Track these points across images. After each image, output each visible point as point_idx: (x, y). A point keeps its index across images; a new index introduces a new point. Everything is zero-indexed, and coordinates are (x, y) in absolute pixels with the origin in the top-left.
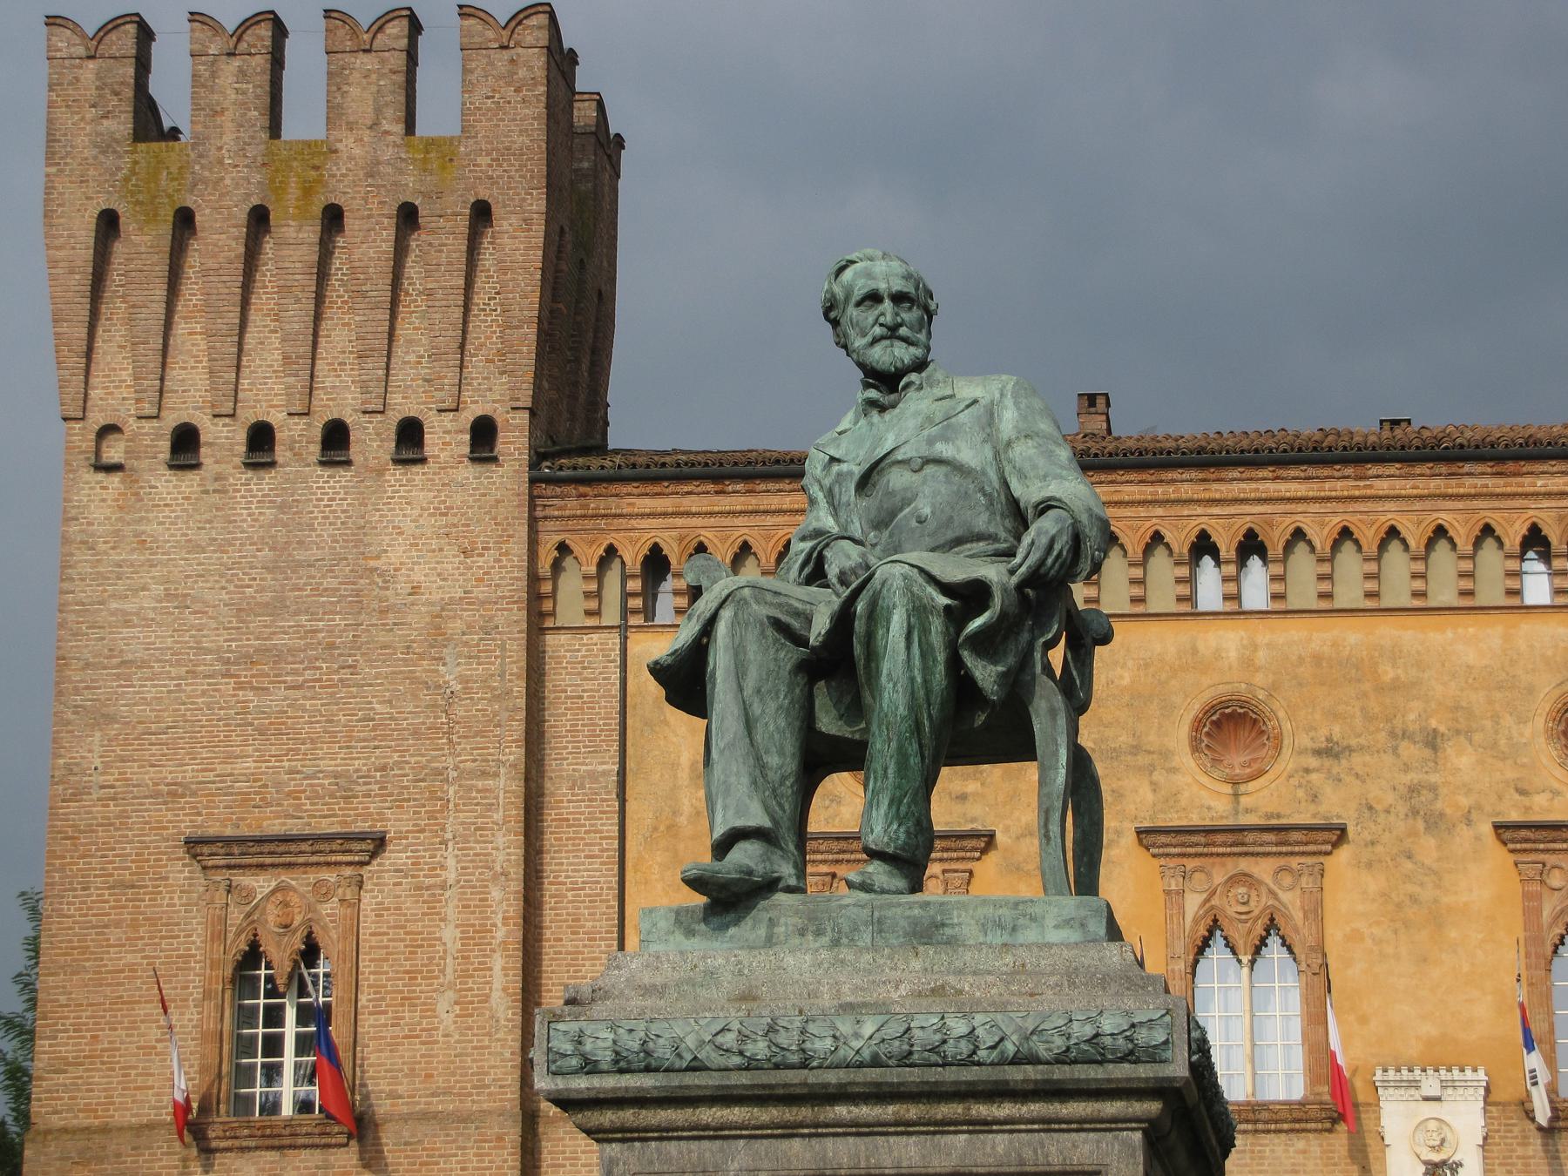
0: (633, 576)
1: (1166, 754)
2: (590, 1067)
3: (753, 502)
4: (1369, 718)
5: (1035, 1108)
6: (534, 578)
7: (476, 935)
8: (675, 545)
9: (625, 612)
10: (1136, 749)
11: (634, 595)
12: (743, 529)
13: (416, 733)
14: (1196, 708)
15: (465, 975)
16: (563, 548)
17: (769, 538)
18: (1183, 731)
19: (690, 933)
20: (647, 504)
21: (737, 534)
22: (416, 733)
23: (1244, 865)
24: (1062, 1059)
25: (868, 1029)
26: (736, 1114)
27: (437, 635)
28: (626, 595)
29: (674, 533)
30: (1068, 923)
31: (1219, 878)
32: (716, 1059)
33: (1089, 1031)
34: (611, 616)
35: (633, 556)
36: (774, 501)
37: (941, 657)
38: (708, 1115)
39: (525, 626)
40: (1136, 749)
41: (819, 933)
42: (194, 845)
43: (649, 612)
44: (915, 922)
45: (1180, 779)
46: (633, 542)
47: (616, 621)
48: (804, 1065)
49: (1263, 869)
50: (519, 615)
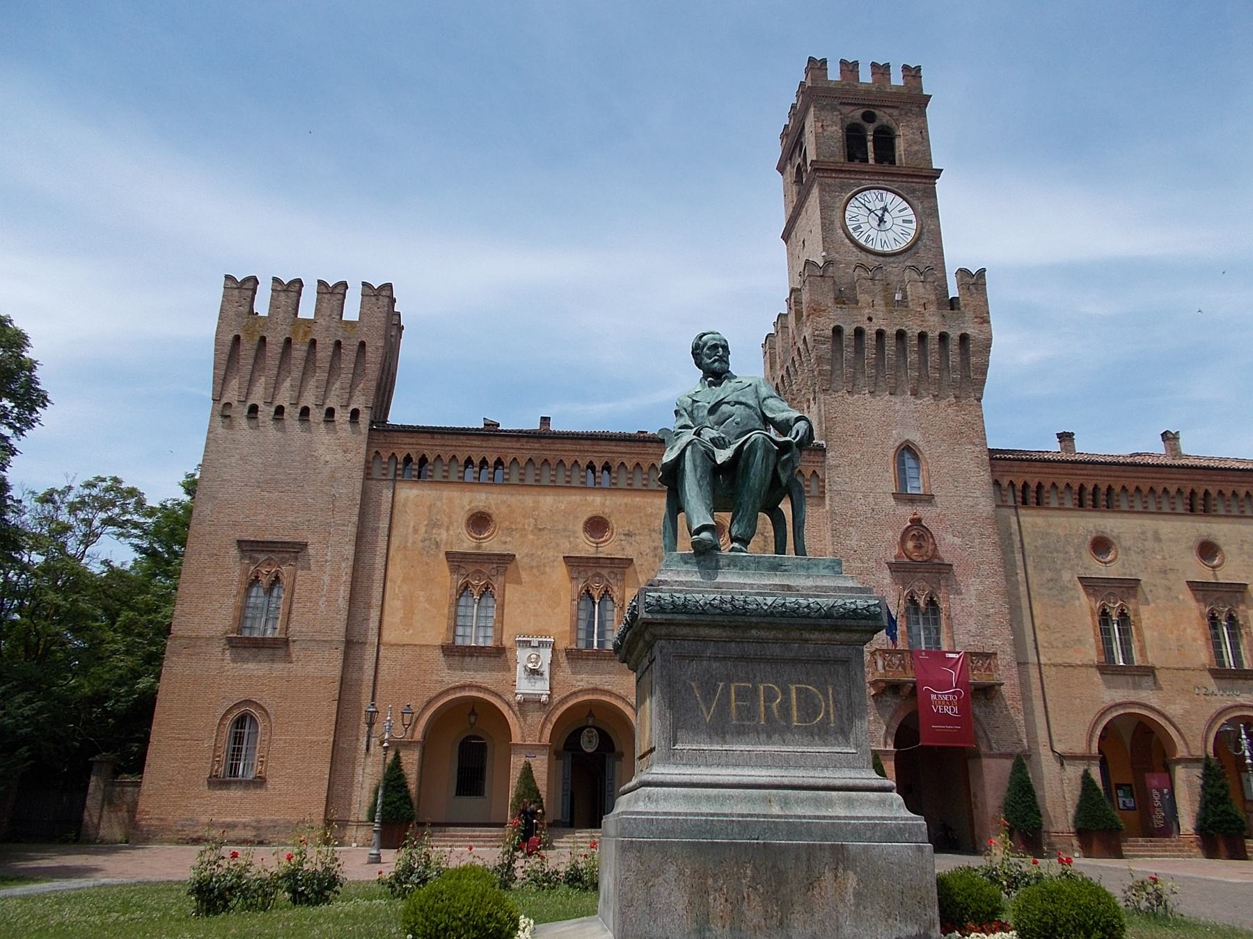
1: (574, 532)
3: (443, 442)
4: (642, 524)
5: (827, 635)
6: (367, 462)
7: (335, 579)
9: (396, 475)
10: (565, 530)
12: (438, 451)
13: (322, 510)
14: (585, 518)
15: (330, 591)
16: (377, 452)
18: (581, 525)
19: (686, 563)
20: (408, 440)
22: (322, 510)
23: (598, 570)
24: (843, 617)
26: (716, 632)
27: (332, 477)
28: (396, 469)
30: (827, 567)
31: (590, 574)
32: (713, 611)
33: (853, 606)
34: (391, 476)
35: (400, 457)
36: (449, 443)
37: (771, 468)
38: (704, 632)
40: (565, 530)
41: (735, 566)
42: (240, 543)
44: (771, 564)
45: (579, 541)
48: (744, 615)
49: (605, 572)
50: (361, 474)
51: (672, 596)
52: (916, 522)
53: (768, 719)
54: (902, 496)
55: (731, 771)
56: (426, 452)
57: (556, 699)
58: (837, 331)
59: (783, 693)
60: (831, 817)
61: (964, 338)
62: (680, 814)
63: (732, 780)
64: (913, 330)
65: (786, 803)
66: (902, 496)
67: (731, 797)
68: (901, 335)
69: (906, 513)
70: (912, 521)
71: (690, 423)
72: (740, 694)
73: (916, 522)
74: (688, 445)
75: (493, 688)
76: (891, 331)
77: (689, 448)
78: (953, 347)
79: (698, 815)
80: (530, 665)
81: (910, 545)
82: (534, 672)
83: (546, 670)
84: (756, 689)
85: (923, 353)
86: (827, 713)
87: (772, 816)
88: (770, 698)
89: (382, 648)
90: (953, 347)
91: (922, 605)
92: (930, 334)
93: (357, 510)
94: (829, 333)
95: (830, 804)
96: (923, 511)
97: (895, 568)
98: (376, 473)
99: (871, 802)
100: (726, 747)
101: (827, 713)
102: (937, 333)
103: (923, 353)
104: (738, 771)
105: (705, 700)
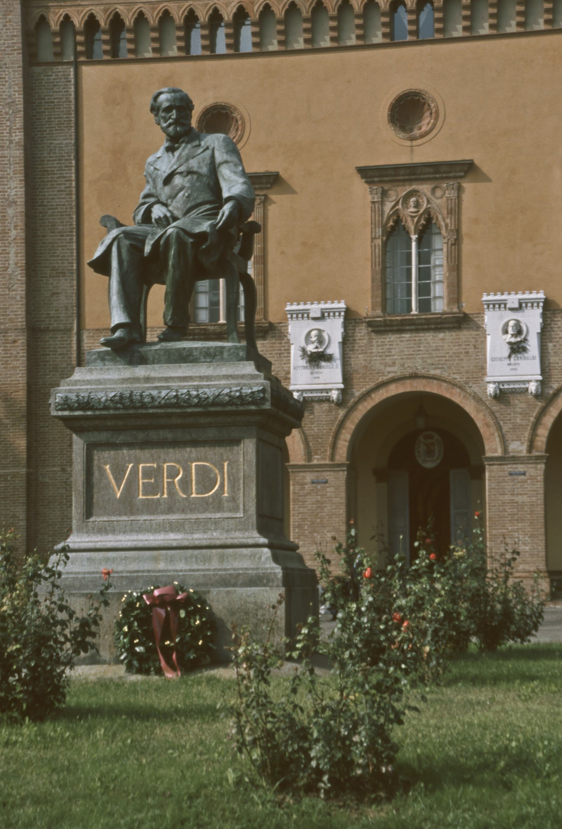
0: (79, 33)
2: (71, 409)
8: (102, 14)
9: (77, 54)
11: (81, 44)
17: (154, 9)
19: (103, 360)
21: (137, 7)
25: (163, 393)
28: (76, 44)
29: (102, 7)
35: (78, 21)
39: (21, 64)
43: (89, 53)
46: (79, 13)
47: (72, 59)
50: (17, 58)
51: (77, 396)
53: (169, 493)
55: (134, 537)
56: (120, 9)
59: (184, 470)
60: (203, 570)
62: (79, 573)
63: (129, 544)
65: (171, 561)
67: (126, 558)
71: (153, 191)
72: (147, 473)
74: (114, 240)
77: (115, 244)
79: (94, 573)
80: (311, 348)
83: (335, 350)
84: (160, 469)
86: (222, 485)
87: (160, 571)
88: (173, 474)
89: (85, 335)
93: (19, 122)
95: (209, 559)
98: (46, 53)
99: (245, 556)
100: (132, 518)
101: (222, 485)
104: (141, 537)
105: (116, 479)
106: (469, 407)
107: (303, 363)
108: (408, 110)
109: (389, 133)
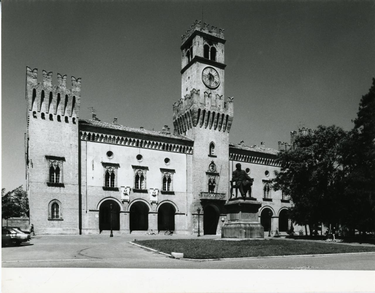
52: (213, 163)
54: (210, 155)
57: (131, 201)
58: (200, 110)
61: (228, 116)
64: (217, 112)
66: (210, 155)
68: (214, 113)
69: (211, 159)
70: (212, 162)
73: (213, 163)
75: (116, 198)
76: (212, 112)
78: (225, 118)
80: (125, 193)
81: (211, 168)
82: (126, 194)
85: (218, 118)
90: (225, 118)
91: (212, 182)
92: (220, 114)
94: (197, 110)
96: (214, 160)
97: (207, 173)
102: (222, 114)
103: (218, 118)
106: (148, 204)
107: (123, 195)
108: (139, 157)
109: (136, 160)
